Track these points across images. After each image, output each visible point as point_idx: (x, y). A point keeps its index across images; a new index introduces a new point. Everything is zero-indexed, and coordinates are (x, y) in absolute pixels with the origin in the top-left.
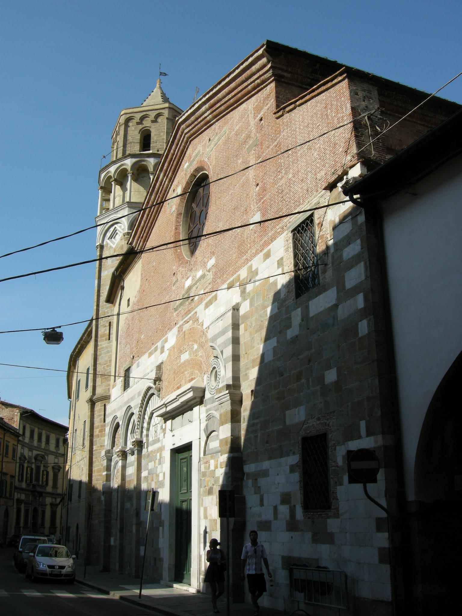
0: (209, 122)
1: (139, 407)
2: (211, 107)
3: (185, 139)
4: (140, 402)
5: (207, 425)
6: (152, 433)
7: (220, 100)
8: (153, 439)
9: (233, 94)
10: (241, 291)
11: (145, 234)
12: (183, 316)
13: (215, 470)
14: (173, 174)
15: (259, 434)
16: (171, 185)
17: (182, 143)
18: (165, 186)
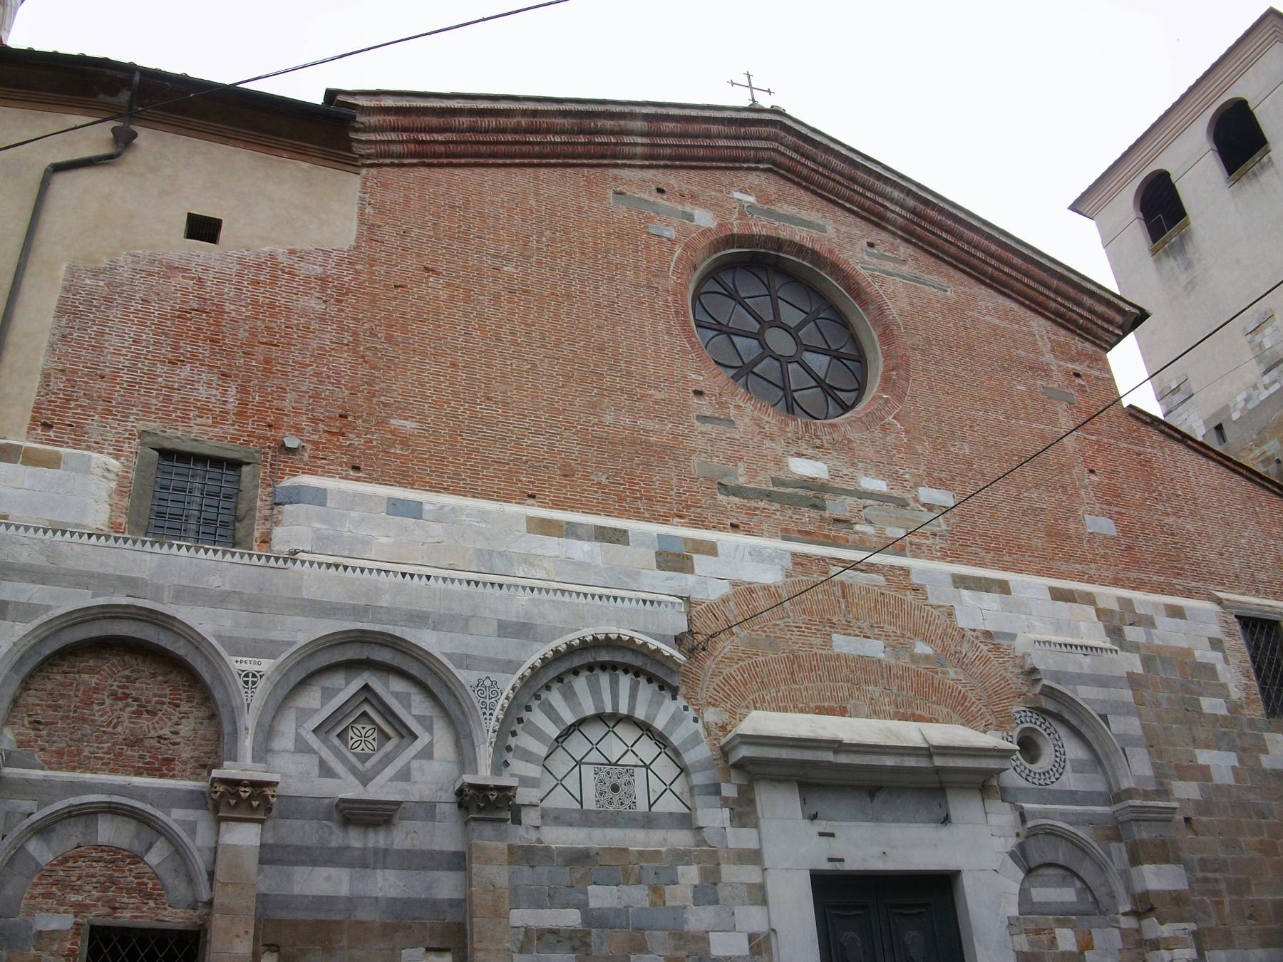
0: (883, 218)
1: (519, 674)
2: (914, 212)
3: (765, 154)
4: (535, 659)
5: (1021, 846)
6: (572, 783)
7: (961, 238)
8: (590, 804)
9: (1041, 289)
10: (1106, 627)
11: (442, 149)
12: (786, 530)
13: (1082, 953)
14: (670, 158)
15: (1226, 900)
16: (642, 167)
17: (750, 148)
18: (626, 150)
